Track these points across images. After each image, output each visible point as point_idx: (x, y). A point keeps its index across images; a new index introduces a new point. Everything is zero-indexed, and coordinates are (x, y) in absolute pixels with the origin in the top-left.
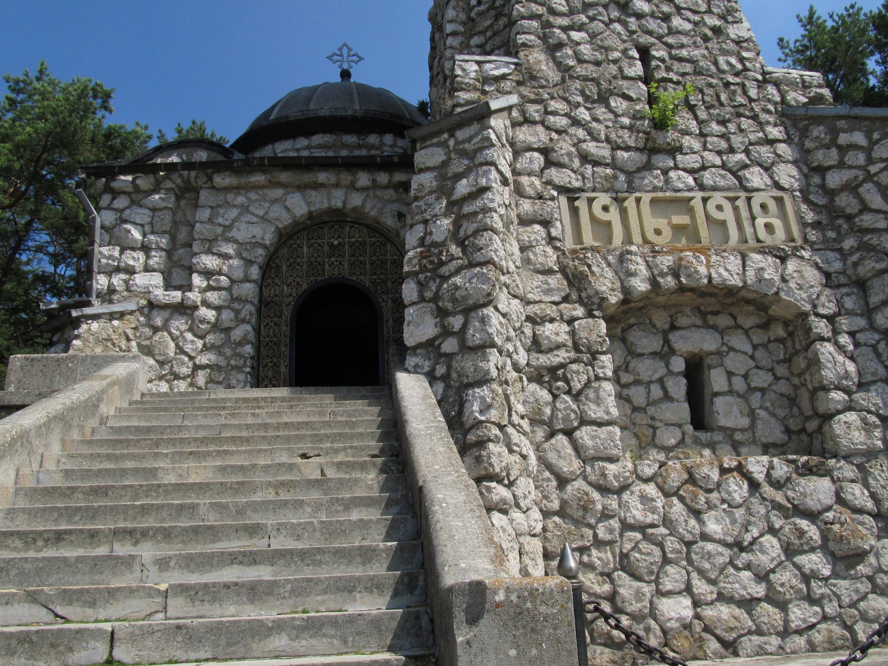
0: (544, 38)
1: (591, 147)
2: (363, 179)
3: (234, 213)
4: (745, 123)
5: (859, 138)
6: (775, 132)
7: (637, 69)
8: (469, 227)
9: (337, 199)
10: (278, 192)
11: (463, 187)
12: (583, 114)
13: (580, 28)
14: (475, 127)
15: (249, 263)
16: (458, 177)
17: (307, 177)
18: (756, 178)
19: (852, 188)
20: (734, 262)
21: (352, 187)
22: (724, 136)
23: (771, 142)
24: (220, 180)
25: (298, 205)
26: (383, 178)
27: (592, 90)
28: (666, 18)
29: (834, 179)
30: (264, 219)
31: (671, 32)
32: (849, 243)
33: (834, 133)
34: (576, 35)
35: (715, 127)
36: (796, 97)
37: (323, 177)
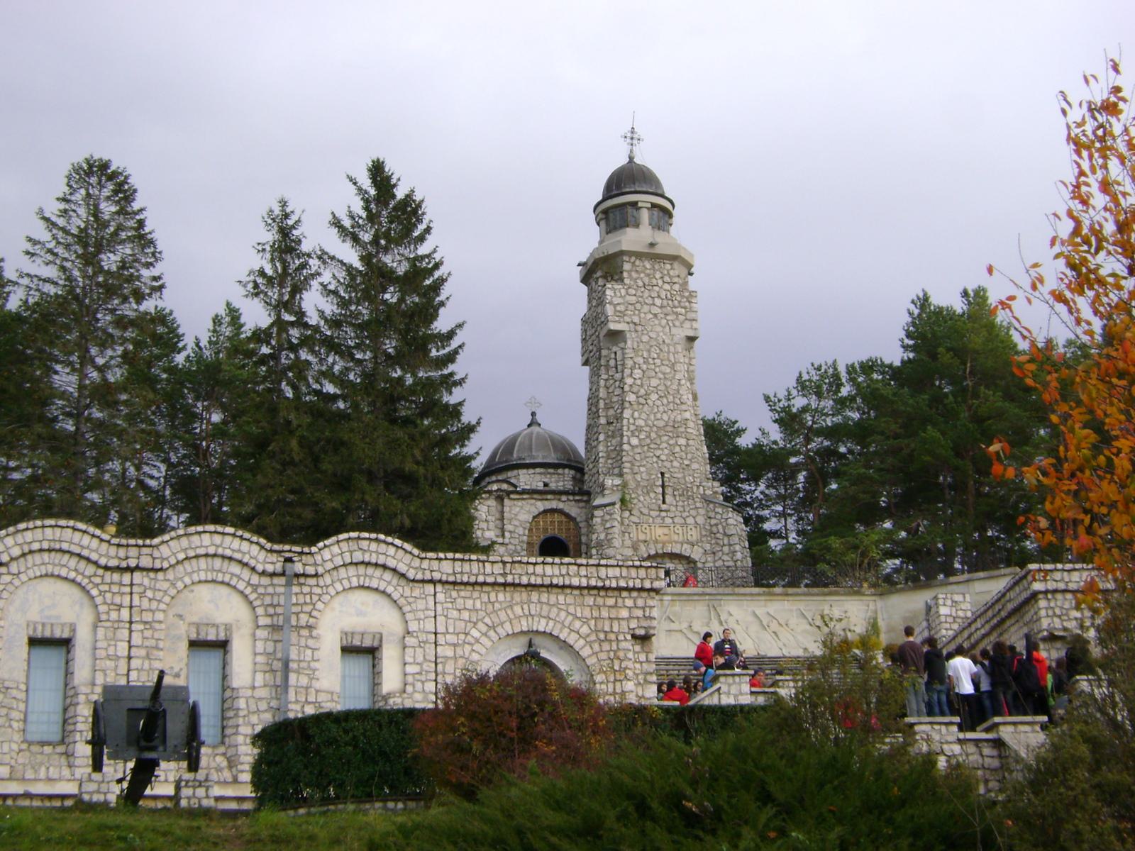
0: (631, 469)
1: (643, 510)
2: (564, 498)
3: (518, 509)
4: (691, 502)
5: (720, 510)
6: (698, 505)
7: (660, 483)
8: (609, 537)
9: (554, 504)
10: (533, 501)
11: (608, 525)
12: (642, 498)
13: (644, 466)
14: (611, 507)
15: (525, 528)
16: (607, 521)
17: (545, 497)
18: (690, 520)
19: (716, 525)
20: (679, 546)
21: (559, 500)
22: (683, 506)
23: (697, 508)
24: (512, 496)
25: (541, 506)
26: (571, 498)
27: (645, 491)
28: (671, 461)
29: (713, 522)
30: (529, 512)
31: (672, 467)
32: (713, 542)
33: (715, 507)
34: (642, 469)
35: (681, 503)
36: (709, 492)
37: (549, 497)
